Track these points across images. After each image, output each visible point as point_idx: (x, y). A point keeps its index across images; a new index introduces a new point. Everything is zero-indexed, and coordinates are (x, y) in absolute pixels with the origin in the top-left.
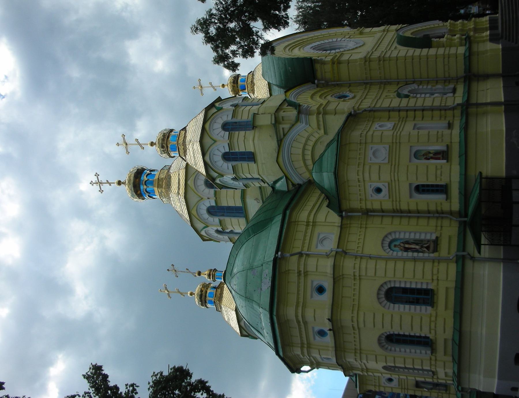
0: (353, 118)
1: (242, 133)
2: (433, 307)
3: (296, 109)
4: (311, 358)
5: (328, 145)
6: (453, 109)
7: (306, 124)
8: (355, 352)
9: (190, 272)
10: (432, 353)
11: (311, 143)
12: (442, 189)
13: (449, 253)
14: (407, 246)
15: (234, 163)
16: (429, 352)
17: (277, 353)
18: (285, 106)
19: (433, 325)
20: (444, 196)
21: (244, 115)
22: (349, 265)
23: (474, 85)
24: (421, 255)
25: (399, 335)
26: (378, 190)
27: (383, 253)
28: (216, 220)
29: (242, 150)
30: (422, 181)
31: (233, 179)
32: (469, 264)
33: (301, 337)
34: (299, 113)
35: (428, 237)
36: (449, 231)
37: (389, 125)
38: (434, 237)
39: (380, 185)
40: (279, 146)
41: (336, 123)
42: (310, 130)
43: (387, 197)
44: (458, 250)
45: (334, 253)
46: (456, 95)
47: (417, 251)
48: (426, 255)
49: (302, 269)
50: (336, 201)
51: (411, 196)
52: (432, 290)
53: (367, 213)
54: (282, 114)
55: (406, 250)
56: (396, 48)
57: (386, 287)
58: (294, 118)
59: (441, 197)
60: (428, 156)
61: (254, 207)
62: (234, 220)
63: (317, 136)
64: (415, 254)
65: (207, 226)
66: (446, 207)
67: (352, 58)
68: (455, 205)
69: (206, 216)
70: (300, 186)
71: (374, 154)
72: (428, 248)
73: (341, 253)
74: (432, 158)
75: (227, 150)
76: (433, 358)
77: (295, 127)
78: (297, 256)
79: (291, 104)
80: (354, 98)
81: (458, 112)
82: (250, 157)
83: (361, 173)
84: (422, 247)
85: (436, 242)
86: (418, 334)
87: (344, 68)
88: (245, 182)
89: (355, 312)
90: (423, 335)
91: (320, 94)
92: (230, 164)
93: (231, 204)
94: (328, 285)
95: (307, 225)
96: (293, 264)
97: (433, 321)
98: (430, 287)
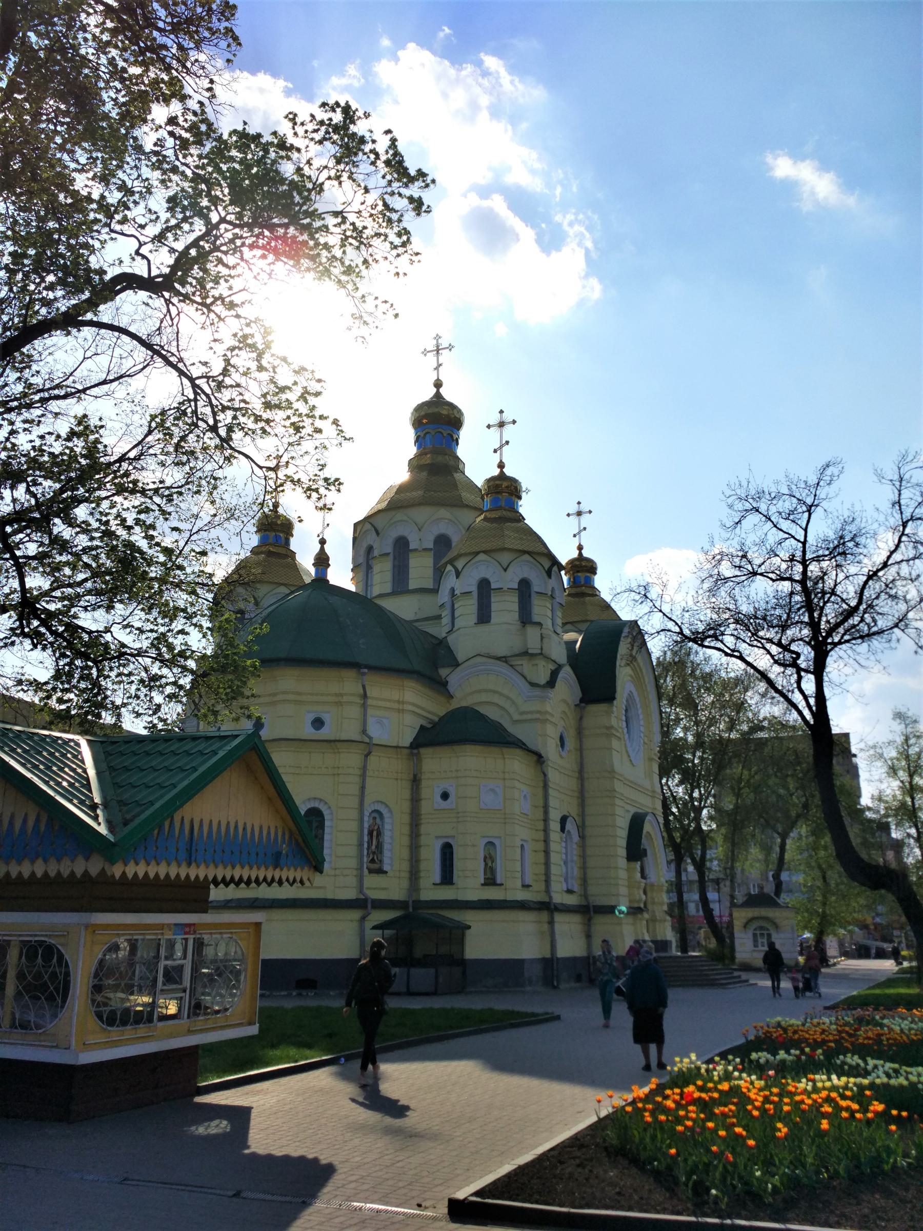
6: (548, 891)
12: (447, 877)
14: (375, 833)
20: (438, 880)
22: (351, 759)
26: (445, 796)
28: (389, 549)
29: (494, 607)
30: (458, 853)
35: (386, 860)
38: (386, 868)
45: (367, 740)
46: (565, 894)
48: (365, 859)
49: (345, 699)
51: (437, 837)
53: (416, 781)
55: (370, 834)
56: (628, 811)
58: (535, 681)
59: (437, 878)
60: (489, 860)
62: (389, 576)
63: (512, 710)
64: (366, 845)
65: (378, 533)
67: (614, 753)
71: (493, 790)
72: (373, 861)
74: (486, 865)
79: (554, 675)
82: (484, 617)
88: (448, 606)
92: (474, 589)
94: (325, 733)
95: (399, 702)
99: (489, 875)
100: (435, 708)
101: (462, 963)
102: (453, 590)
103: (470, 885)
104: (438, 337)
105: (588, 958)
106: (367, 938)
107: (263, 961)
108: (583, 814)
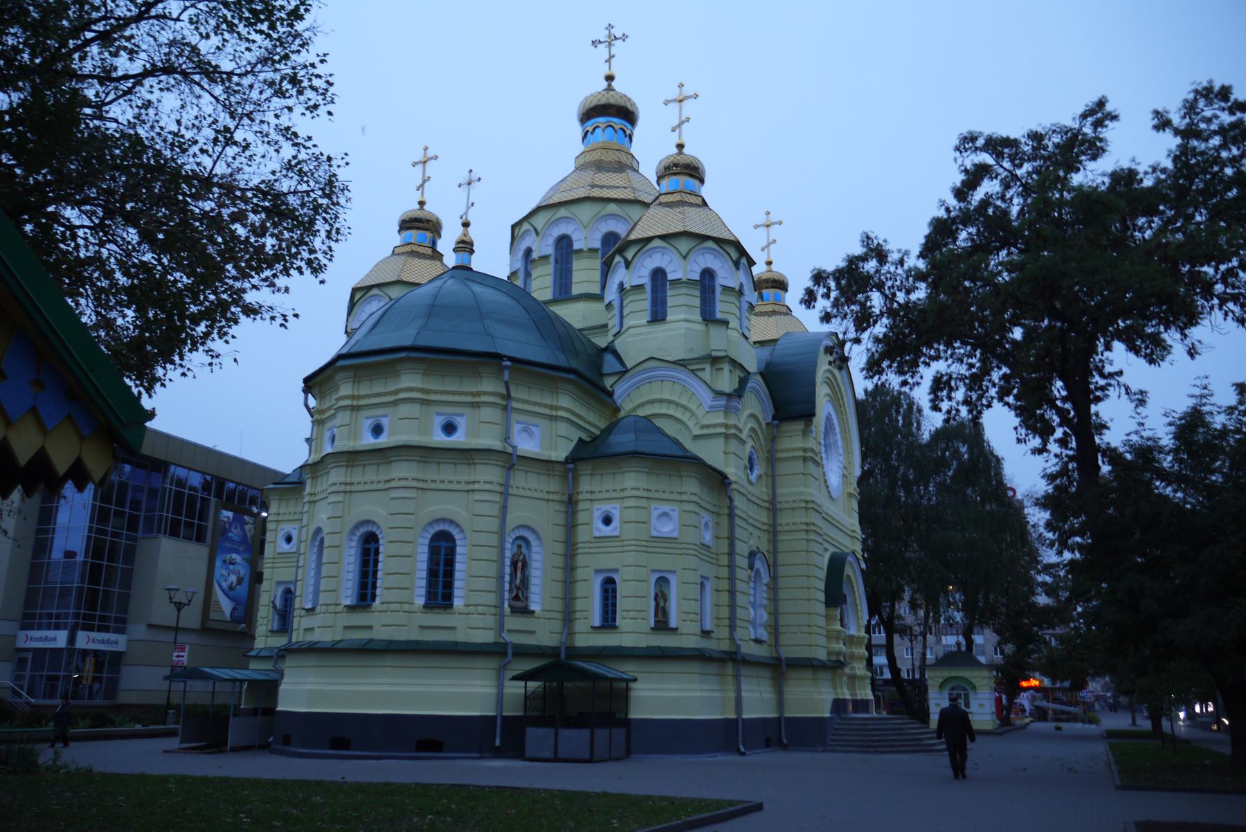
0: (718, 481)
1: (697, 302)
2: (426, 606)
3: (735, 391)
4: (332, 412)
5: (676, 442)
6: (732, 639)
7: (711, 407)
8: (346, 484)
9: (468, 208)
10: (348, 607)
11: (678, 414)
12: (609, 620)
13: (509, 631)
14: (520, 565)
15: (648, 288)
16: (348, 602)
17: (339, 357)
18: (738, 372)
19: (392, 606)
20: (597, 623)
21: (723, 307)
22: (488, 474)
23: (766, 673)
24: (507, 586)
25: (377, 552)
27: (510, 525)
29: (670, 302)
30: (622, 589)
31: (621, 284)
32: (494, 663)
33: (369, 396)
34: (729, 396)
36: (543, 631)
37: (708, 537)
38: (533, 607)
39: (615, 523)
40: (674, 363)
41: (712, 453)
42: (700, 413)
43: (597, 534)
44: (516, 646)
45: (510, 450)
46: (752, 643)
47: (511, 583)
48: (507, 595)
50: (591, 453)
51: (598, 571)
52: (451, 606)
53: (571, 504)
54: (726, 367)
55: (514, 564)
56: (826, 550)
57: (454, 532)
60: (661, 598)
61: (574, 315)
63: (691, 424)
64: (507, 578)
66: (580, 626)
68: (585, 640)
69: (557, 232)
70: (611, 394)
71: (665, 514)
72: (517, 598)
73: (510, 461)
74: (657, 605)
75: (670, 277)
76: (340, 608)
77: (705, 387)
78: (504, 392)
79: (743, 382)
80: (750, 482)
81: (725, 646)
82: (658, 315)
83: (634, 493)
84: (518, 588)
86: (379, 583)
87: (798, 466)
88: (616, 304)
89: (415, 484)
90: (378, 591)
91: (756, 427)
92: (645, 280)
93: (576, 276)
94: (459, 439)
96: (489, 386)
97: (401, 608)
98: (458, 602)
99: (660, 618)
100: (596, 421)
101: (626, 723)
102: (621, 284)
103: (633, 630)
104: (610, 26)
105: (779, 718)
106: (506, 691)
108: (775, 552)
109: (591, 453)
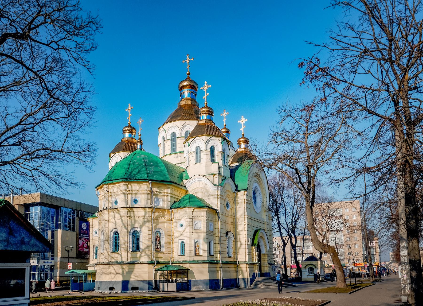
12: (183, 253)
15: (196, 152)
65: (165, 132)
82: (198, 161)
85: (160, 252)
92: (194, 150)
107: (25, 269)
109: (176, 205)
